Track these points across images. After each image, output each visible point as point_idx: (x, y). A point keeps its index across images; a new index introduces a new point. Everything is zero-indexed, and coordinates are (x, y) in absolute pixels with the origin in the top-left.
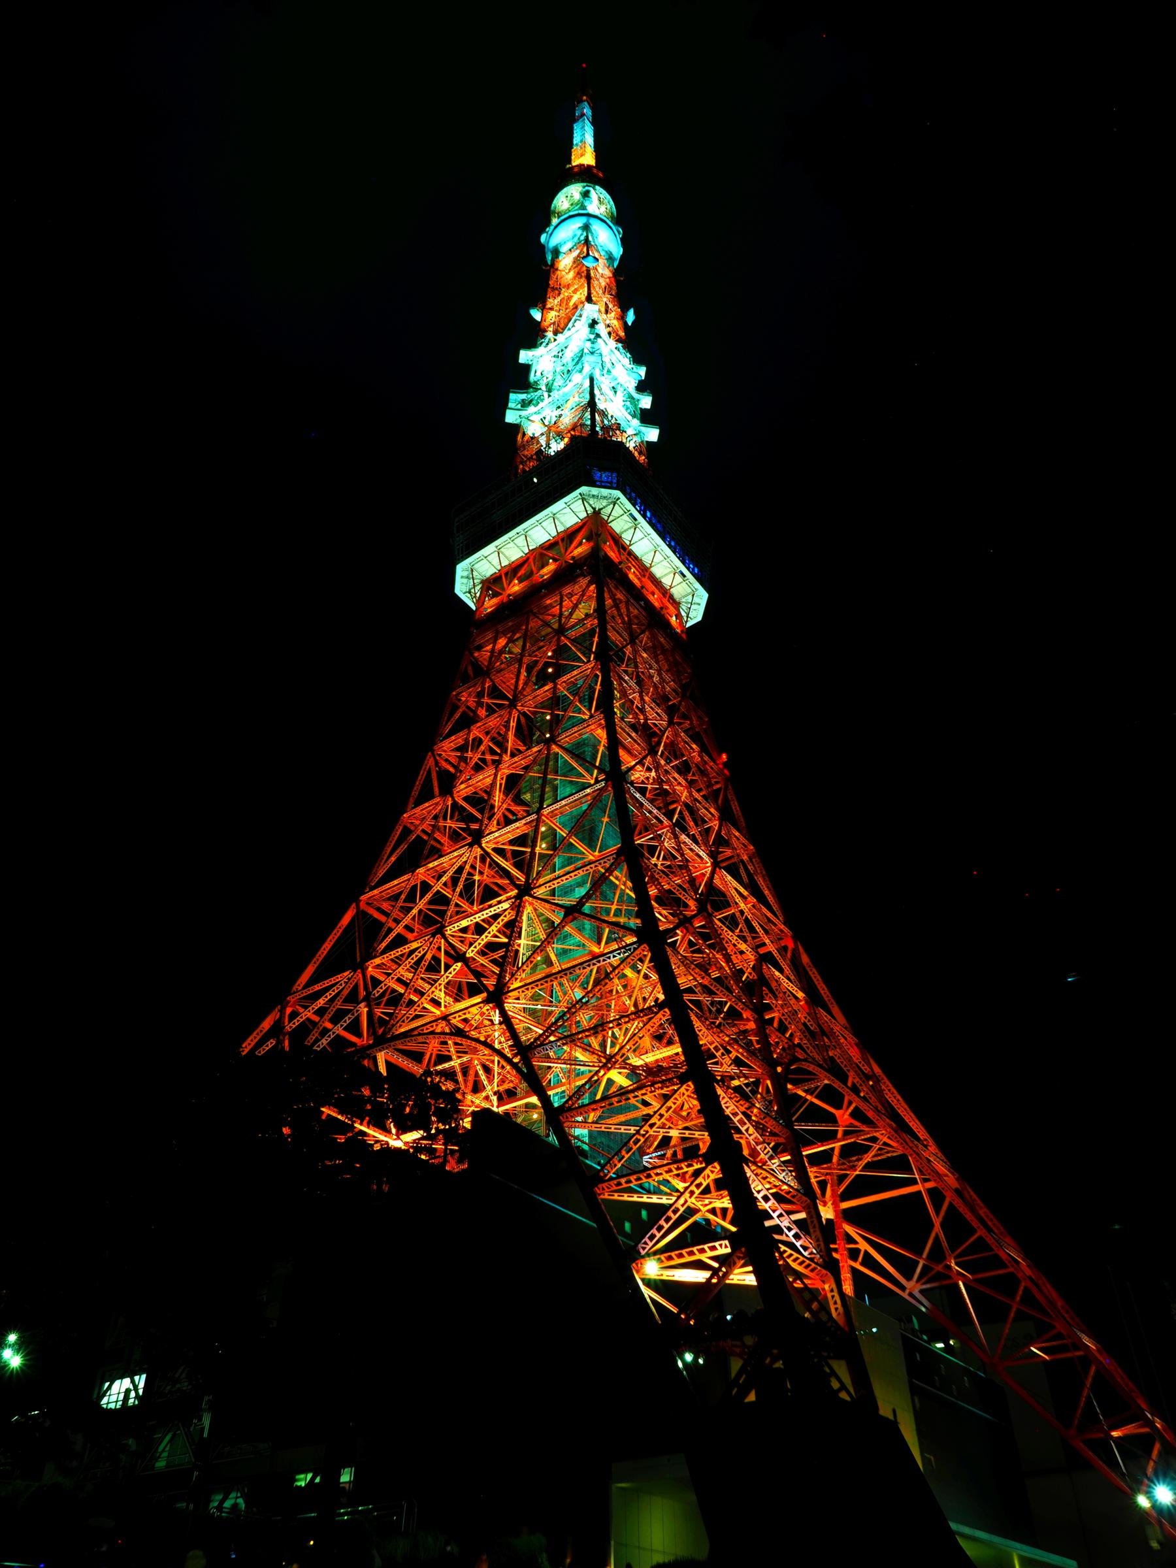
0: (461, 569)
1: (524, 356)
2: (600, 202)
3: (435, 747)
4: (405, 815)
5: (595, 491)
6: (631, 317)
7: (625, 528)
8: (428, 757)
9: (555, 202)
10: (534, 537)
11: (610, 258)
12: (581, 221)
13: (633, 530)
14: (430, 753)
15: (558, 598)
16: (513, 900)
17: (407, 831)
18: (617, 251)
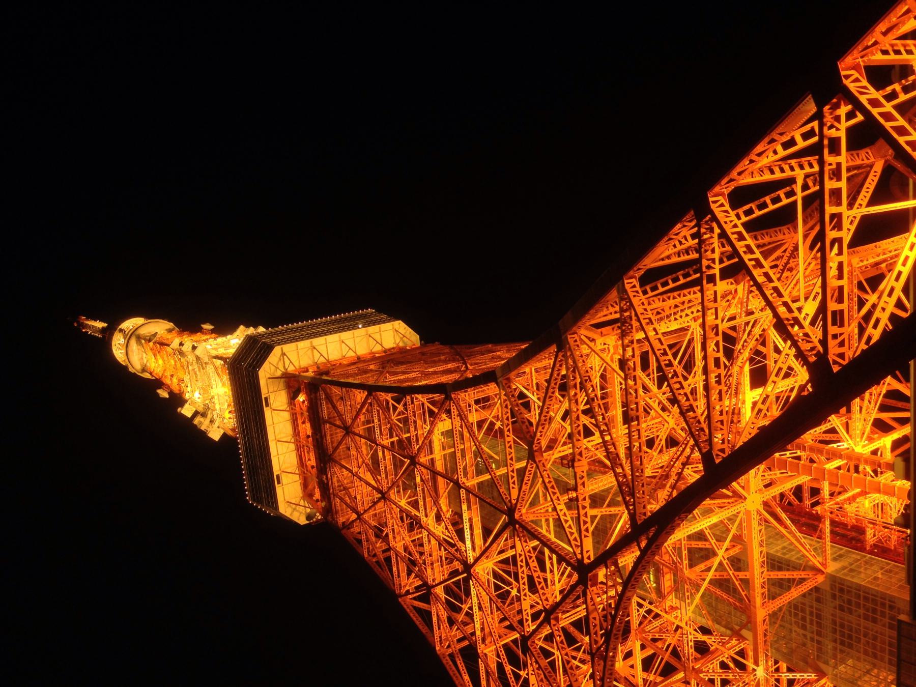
0: (284, 509)
1: (187, 411)
2: (129, 324)
3: (397, 592)
4: (437, 648)
5: (266, 365)
6: (207, 327)
7: (311, 357)
8: (403, 603)
9: (120, 360)
10: (283, 435)
11: (170, 331)
12: (133, 342)
13: (315, 351)
14: (400, 600)
15: (328, 426)
16: (516, 533)
17: (452, 656)
18: (170, 325)
